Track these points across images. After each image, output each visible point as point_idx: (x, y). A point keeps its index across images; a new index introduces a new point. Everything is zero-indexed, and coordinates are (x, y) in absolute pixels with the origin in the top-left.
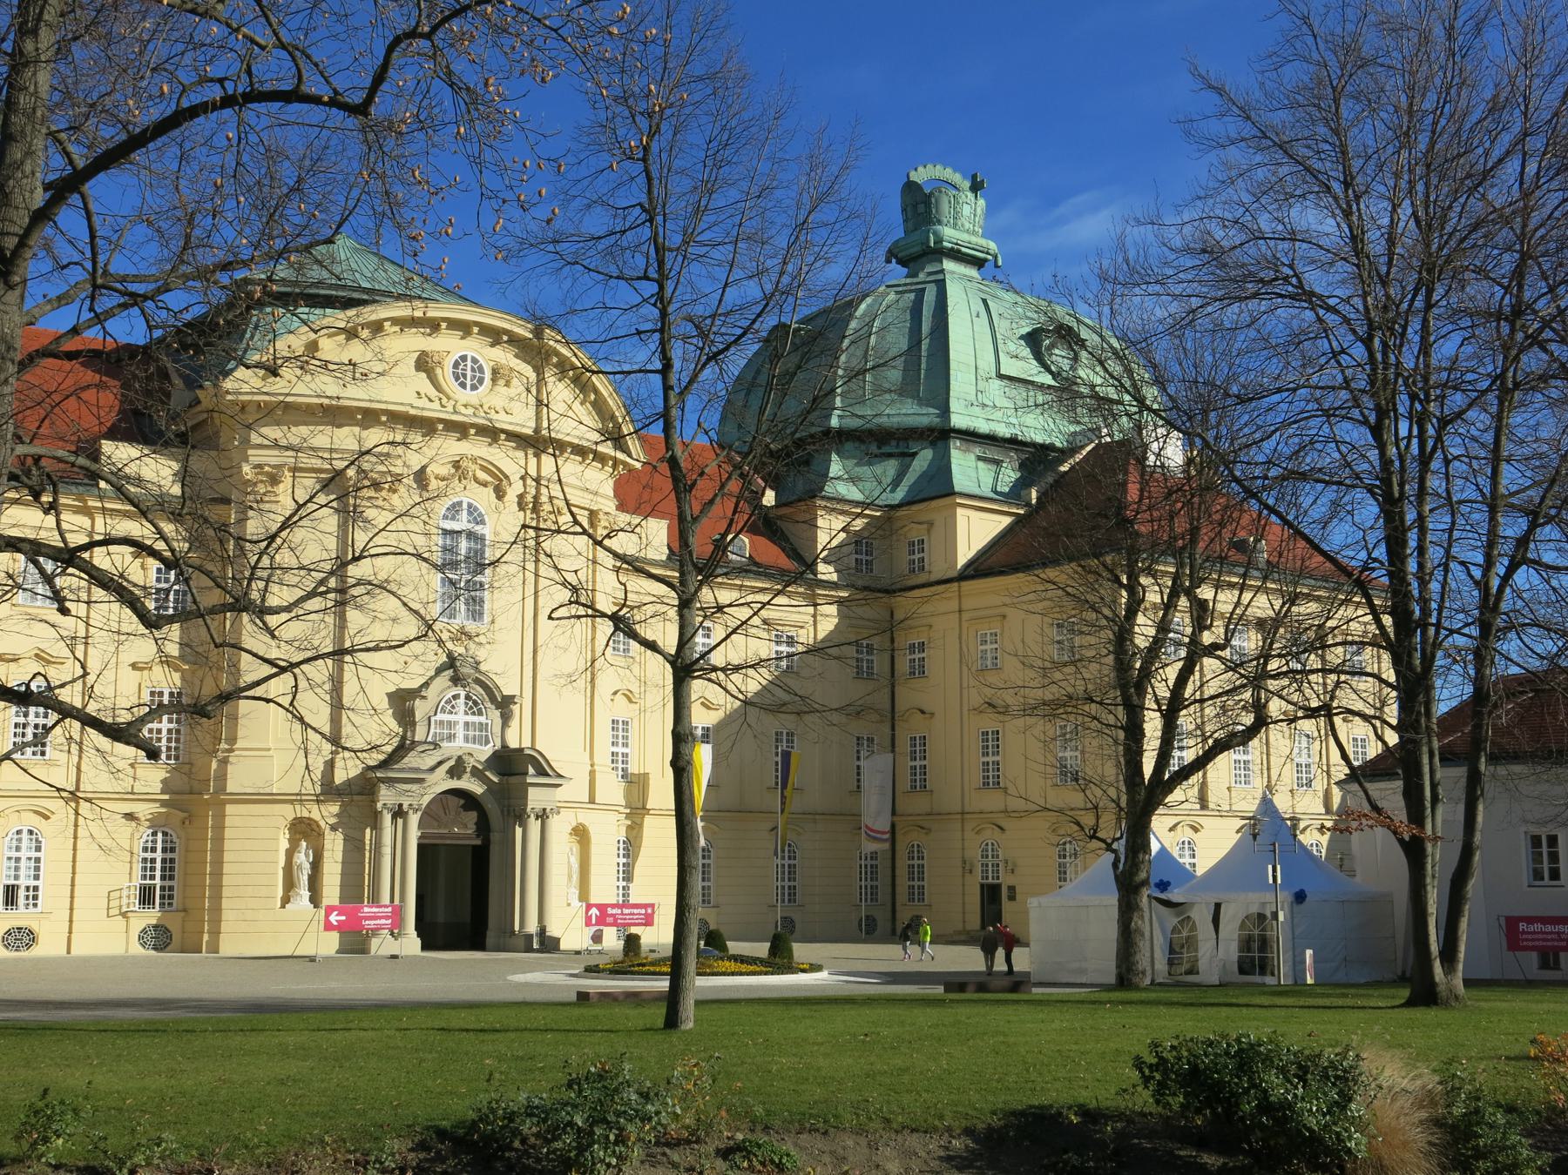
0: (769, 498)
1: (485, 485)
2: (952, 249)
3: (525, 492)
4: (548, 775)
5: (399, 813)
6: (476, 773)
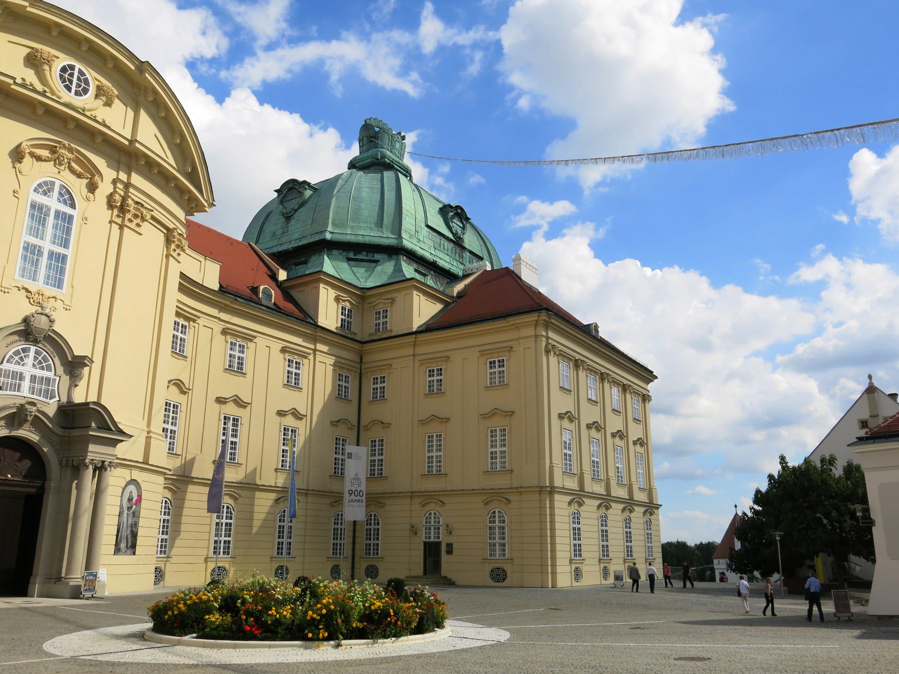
0: (282, 275)
1: (79, 176)
2: (390, 163)
3: (115, 192)
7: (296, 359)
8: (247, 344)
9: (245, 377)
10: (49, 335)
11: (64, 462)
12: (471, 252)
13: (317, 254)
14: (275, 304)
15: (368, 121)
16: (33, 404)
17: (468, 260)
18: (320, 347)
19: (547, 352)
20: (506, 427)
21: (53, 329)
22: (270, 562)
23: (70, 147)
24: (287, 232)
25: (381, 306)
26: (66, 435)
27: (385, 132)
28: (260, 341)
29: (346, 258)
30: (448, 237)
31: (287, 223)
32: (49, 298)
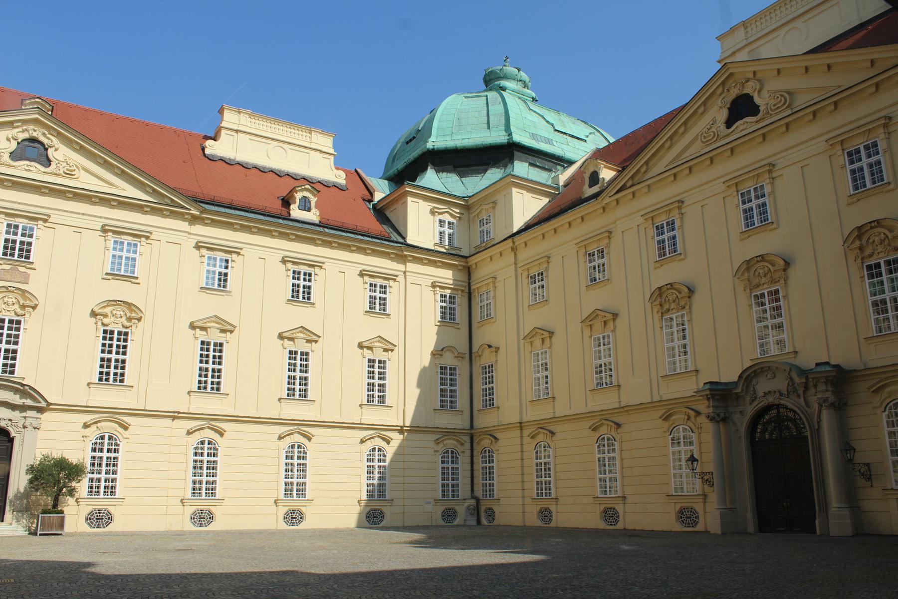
18: (411, 267)
25: (484, 212)
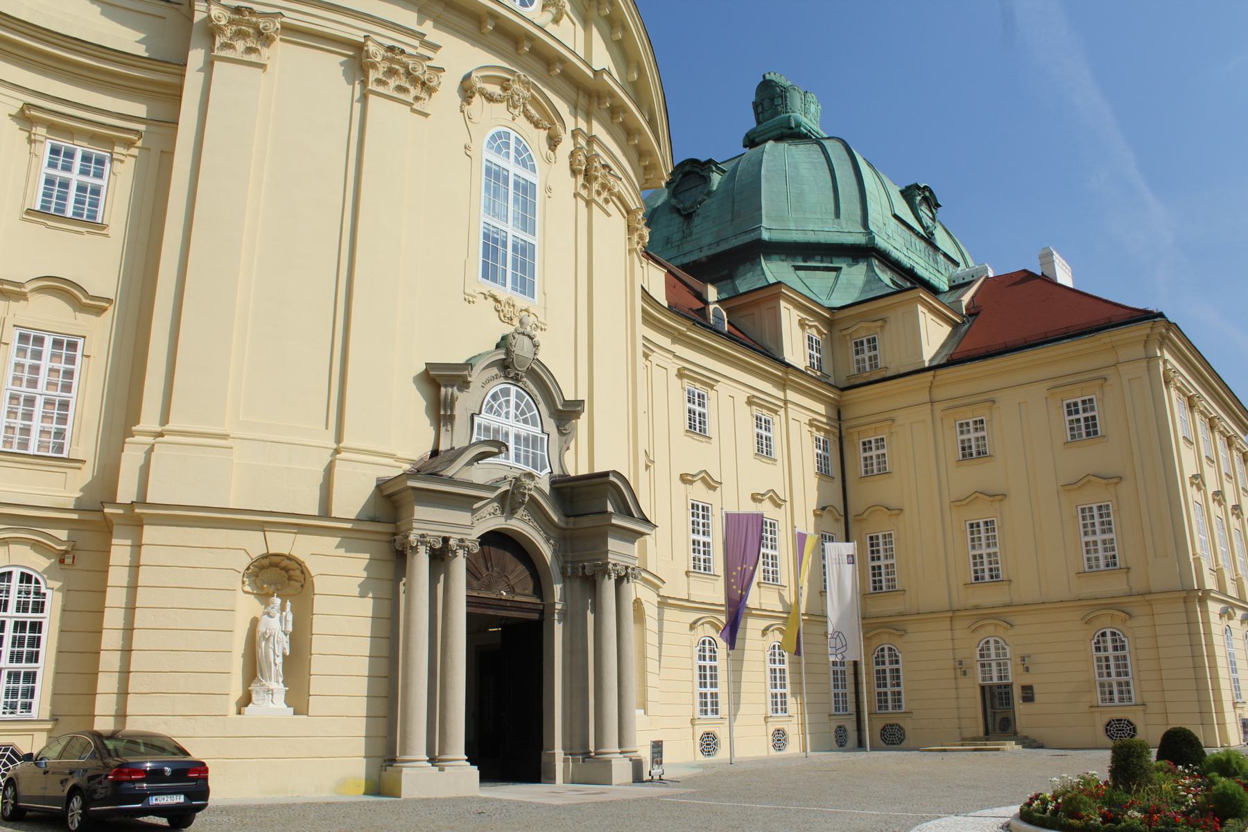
1: (537, 125)
2: (807, 134)
4: (631, 515)
5: (440, 557)
6: (535, 508)
7: (766, 415)
8: (707, 393)
9: (711, 443)
10: (532, 368)
11: (569, 570)
12: (945, 255)
13: (749, 263)
14: (729, 332)
15: (767, 76)
16: (530, 476)
17: (943, 268)
18: (792, 395)
19: (1167, 383)
20: (1110, 503)
21: (537, 359)
22: (828, 721)
23: (525, 83)
24: (689, 236)
26: (571, 526)
27: (795, 89)
28: (723, 387)
29: (793, 266)
30: (919, 233)
31: (689, 224)
32: (521, 311)
